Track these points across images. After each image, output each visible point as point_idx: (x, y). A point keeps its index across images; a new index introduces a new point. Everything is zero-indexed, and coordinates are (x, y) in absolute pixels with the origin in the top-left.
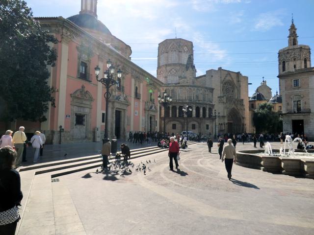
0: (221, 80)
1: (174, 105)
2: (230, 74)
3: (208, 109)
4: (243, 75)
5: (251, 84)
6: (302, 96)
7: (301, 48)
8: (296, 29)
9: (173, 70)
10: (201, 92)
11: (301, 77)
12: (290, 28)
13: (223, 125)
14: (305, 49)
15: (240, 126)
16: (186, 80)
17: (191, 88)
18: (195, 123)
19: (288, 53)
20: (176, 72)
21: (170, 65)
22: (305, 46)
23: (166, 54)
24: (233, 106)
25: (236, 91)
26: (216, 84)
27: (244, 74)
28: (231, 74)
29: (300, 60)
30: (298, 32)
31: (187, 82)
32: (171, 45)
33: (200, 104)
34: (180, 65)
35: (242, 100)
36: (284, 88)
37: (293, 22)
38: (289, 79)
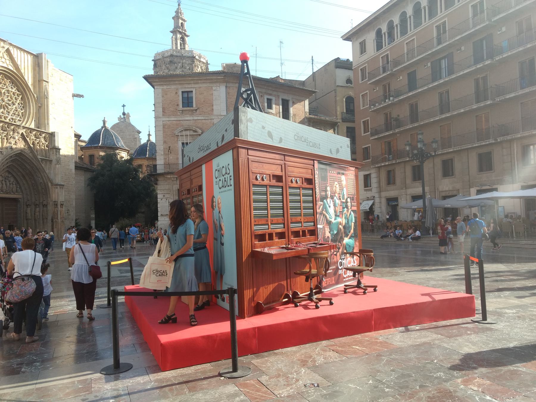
2: (8, 51)
5: (81, 96)
6: (200, 132)
7: (195, 57)
8: (184, 20)
11: (196, 86)
12: (174, 14)
14: (200, 61)
15: (45, 206)
19: (171, 62)
28: (15, 53)
36: (161, 110)
37: (179, 5)
38: (173, 87)
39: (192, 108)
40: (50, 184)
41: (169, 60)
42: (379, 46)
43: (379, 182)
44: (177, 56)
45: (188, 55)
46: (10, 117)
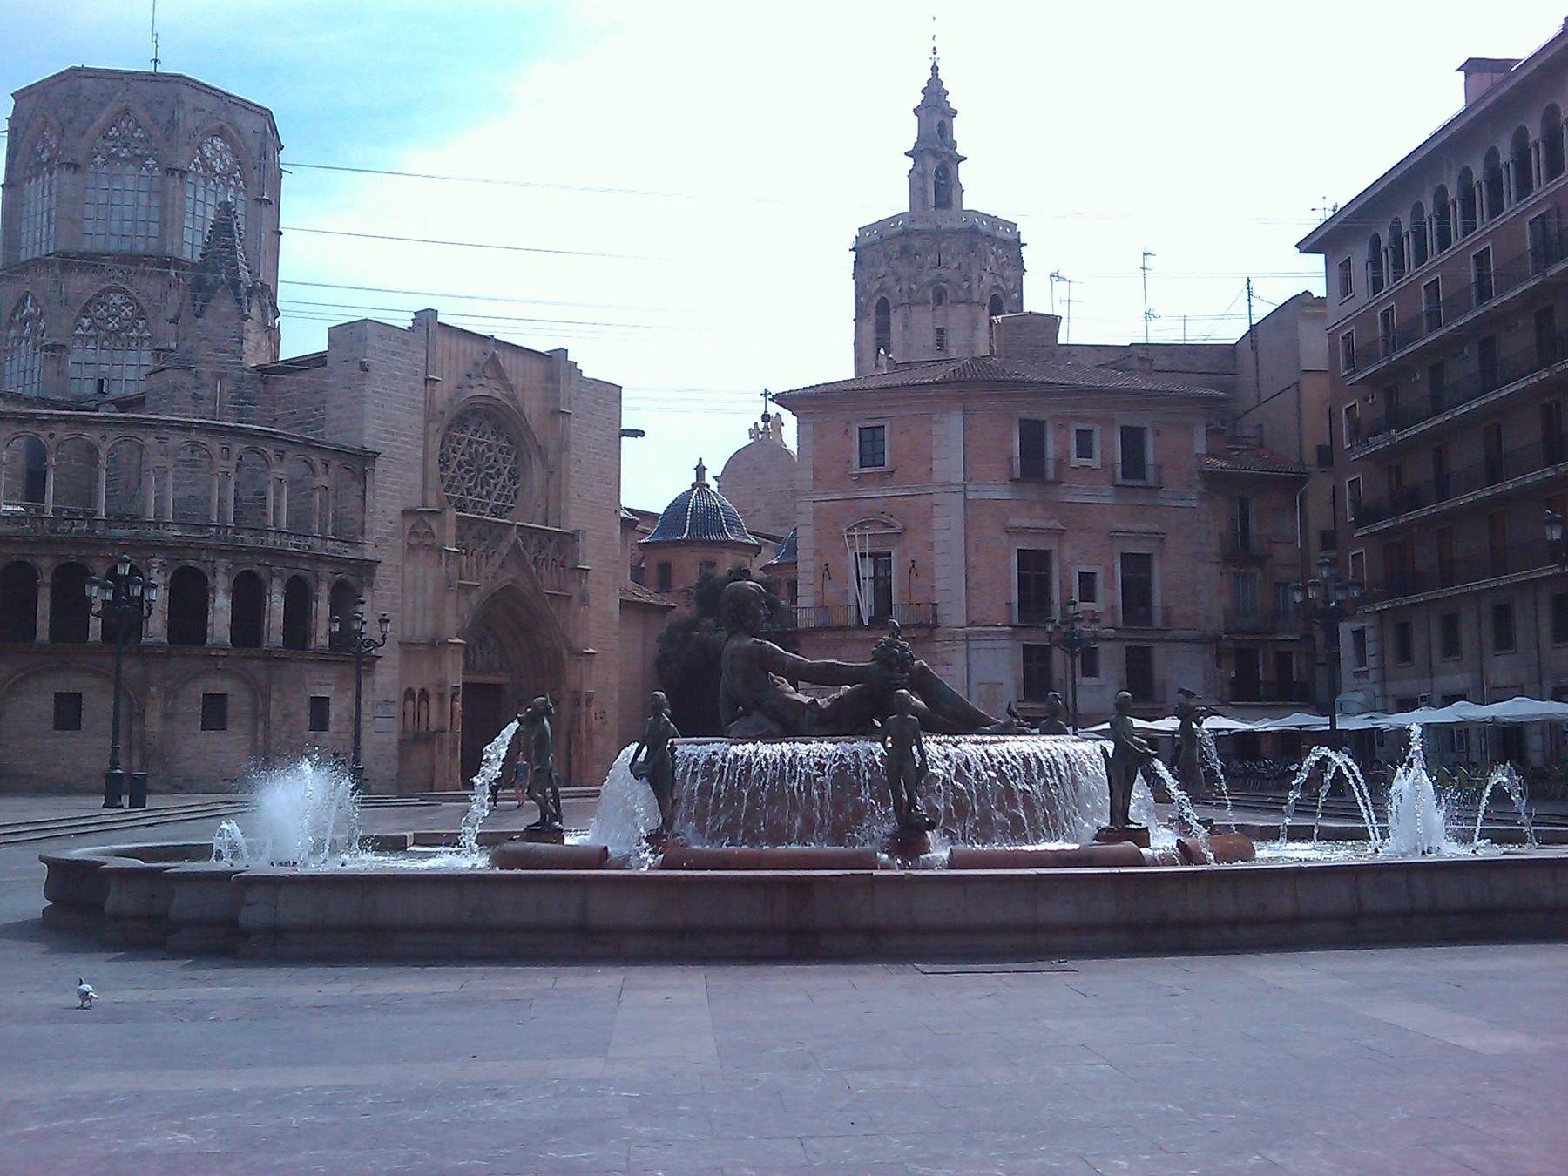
0: (429, 403)
1: (72, 554)
2: (494, 358)
3: (324, 591)
4: (588, 373)
5: (642, 434)
7: (974, 231)
9: (116, 299)
10: (279, 471)
12: (918, 98)
13: (434, 704)
16: (189, 380)
17: (204, 439)
18: (224, 685)
19: (905, 251)
20: (141, 314)
21: (91, 261)
22: (994, 221)
23: (67, 177)
24: (506, 578)
25: (536, 475)
26: (394, 426)
27: (592, 365)
28: (506, 360)
29: (968, 302)
30: (963, 133)
31: (196, 398)
32: (103, 118)
33: (267, 553)
34: (164, 262)
35: (574, 536)
37: (935, 69)
39: (882, 469)
40: (565, 652)
41: (897, 247)
42: (1377, 285)
43: (1382, 654)
44: (920, 233)
45: (957, 226)
46: (492, 503)
